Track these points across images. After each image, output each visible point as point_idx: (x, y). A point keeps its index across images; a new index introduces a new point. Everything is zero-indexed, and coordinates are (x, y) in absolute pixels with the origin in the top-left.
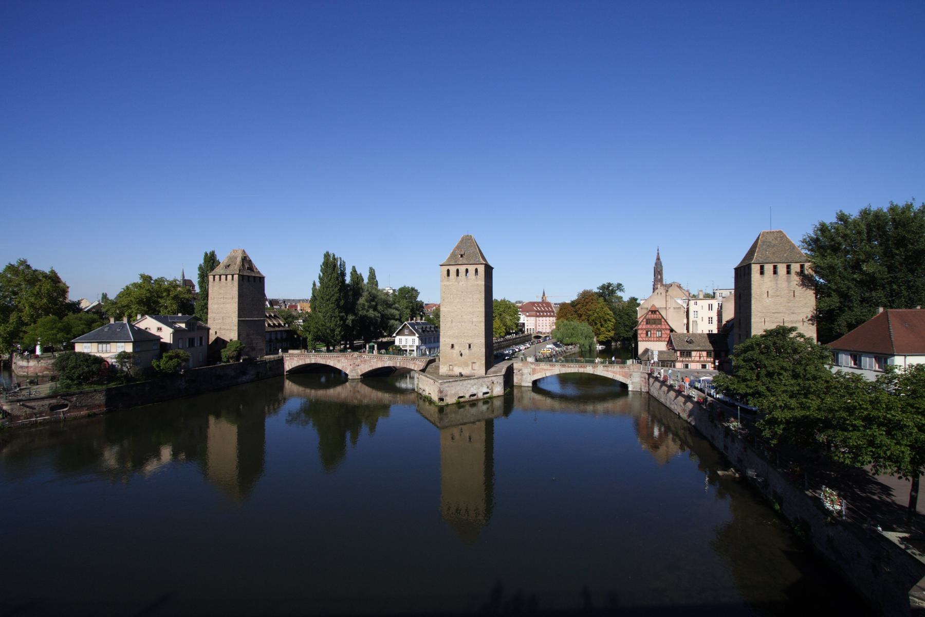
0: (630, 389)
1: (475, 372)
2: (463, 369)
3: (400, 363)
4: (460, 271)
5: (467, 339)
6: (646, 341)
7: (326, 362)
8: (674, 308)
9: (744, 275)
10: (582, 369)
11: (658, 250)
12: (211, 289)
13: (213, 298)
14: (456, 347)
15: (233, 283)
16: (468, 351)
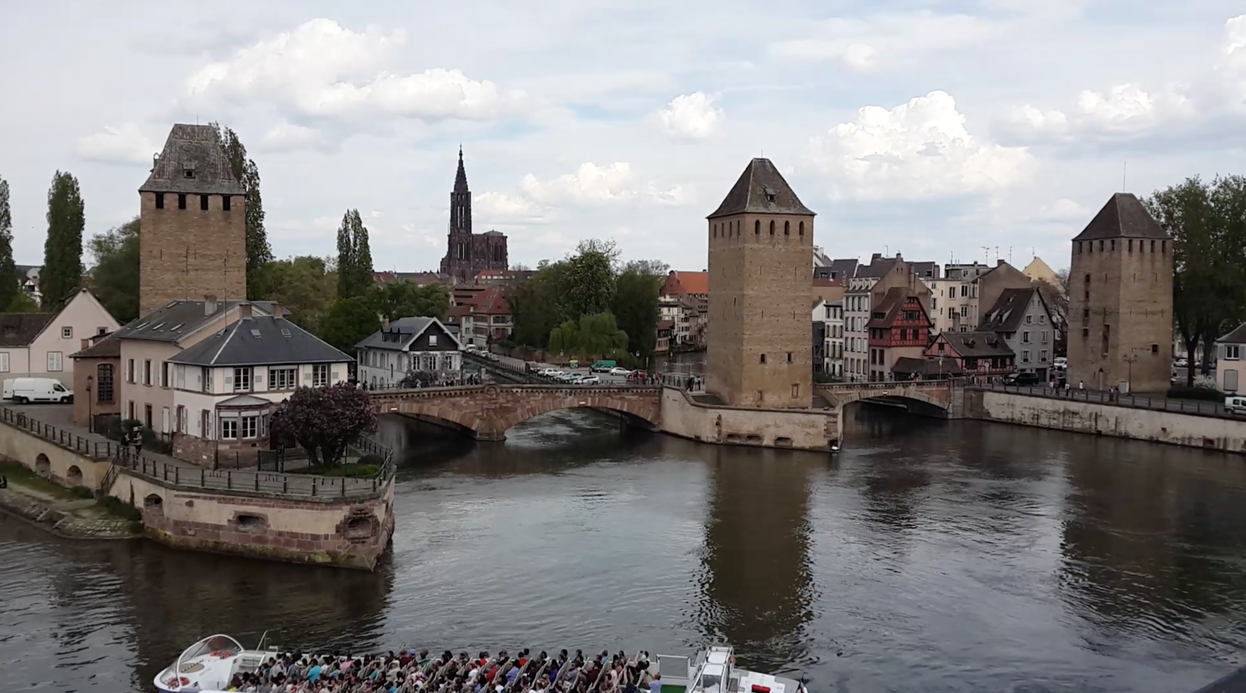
0: (950, 417)
1: (798, 400)
2: (780, 397)
3: (593, 401)
4: (776, 225)
5: (786, 346)
6: (900, 346)
7: (421, 409)
8: (920, 294)
9: (1102, 250)
10: (890, 390)
11: (461, 155)
12: (151, 228)
13: (156, 252)
14: (769, 360)
15: (227, 218)
16: (786, 365)
